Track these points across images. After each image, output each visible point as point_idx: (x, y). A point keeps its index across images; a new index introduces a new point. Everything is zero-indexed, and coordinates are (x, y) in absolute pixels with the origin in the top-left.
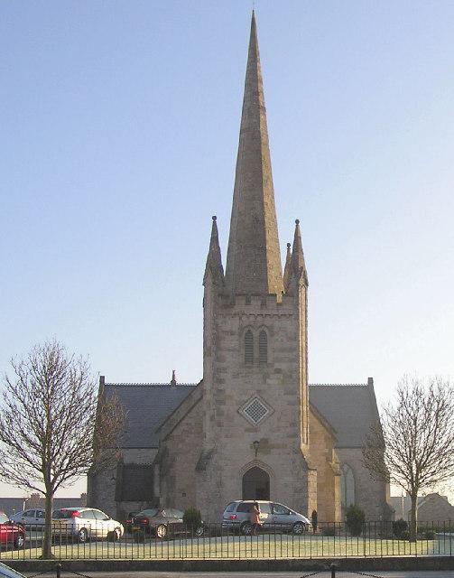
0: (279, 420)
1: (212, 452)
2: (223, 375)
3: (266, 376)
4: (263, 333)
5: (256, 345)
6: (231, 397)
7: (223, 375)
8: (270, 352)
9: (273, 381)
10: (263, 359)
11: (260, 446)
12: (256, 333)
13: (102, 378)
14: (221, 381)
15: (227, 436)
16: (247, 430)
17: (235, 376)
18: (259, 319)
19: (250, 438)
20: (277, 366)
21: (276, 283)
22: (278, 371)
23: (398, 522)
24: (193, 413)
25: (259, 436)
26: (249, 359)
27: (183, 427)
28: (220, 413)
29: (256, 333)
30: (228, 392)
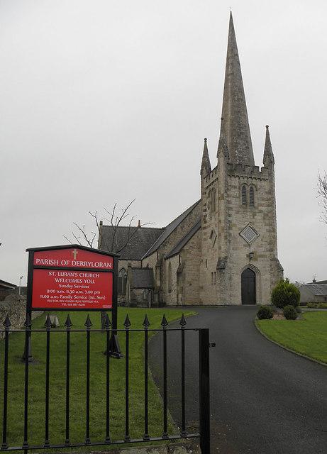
0: (262, 240)
1: (226, 258)
2: (231, 212)
3: (254, 215)
4: (251, 188)
5: (248, 195)
6: (235, 225)
7: (231, 212)
8: (256, 199)
9: (259, 217)
10: (252, 203)
11: (251, 256)
12: (248, 189)
13: (101, 222)
14: (230, 215)
15: (233, 249)
16: (245, 246)
17: (237, 213)
18: (250, 180)
19: (246, 251)
20: (260, 208)
21: (259, 161)
22: (261, 212)
23: (273, 300)
24: (195, 237)
25: (252, 250)
26: (244, 202)
27: (190, 244)
28: (230, 235)
29: (248, 189)
30: (233, 222)
